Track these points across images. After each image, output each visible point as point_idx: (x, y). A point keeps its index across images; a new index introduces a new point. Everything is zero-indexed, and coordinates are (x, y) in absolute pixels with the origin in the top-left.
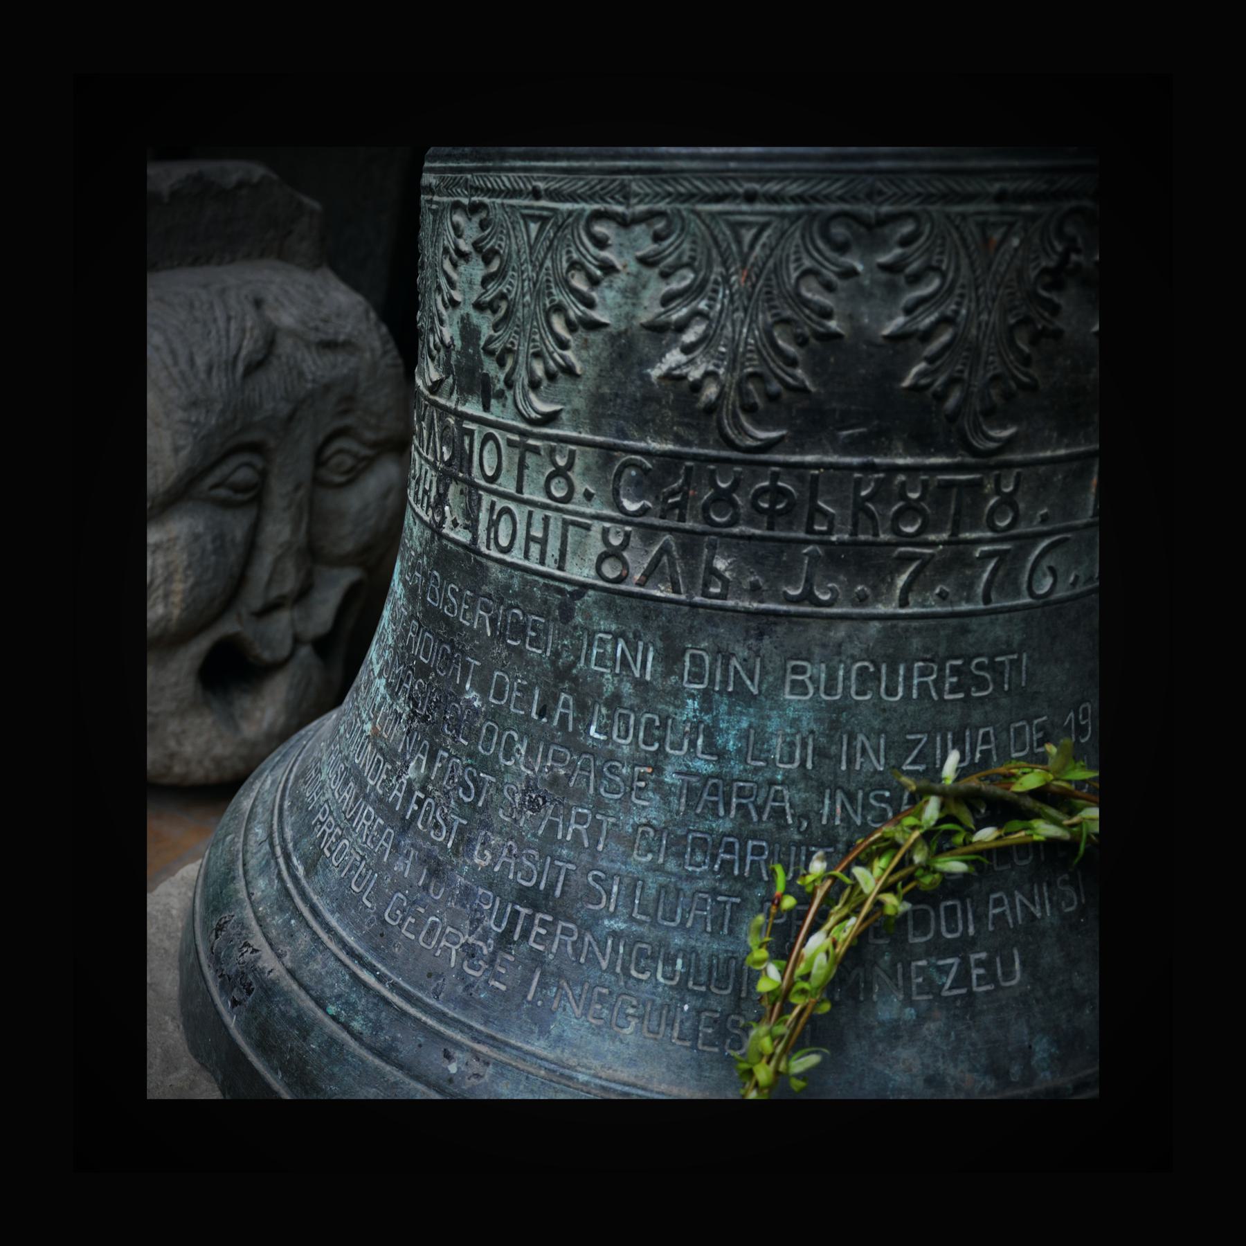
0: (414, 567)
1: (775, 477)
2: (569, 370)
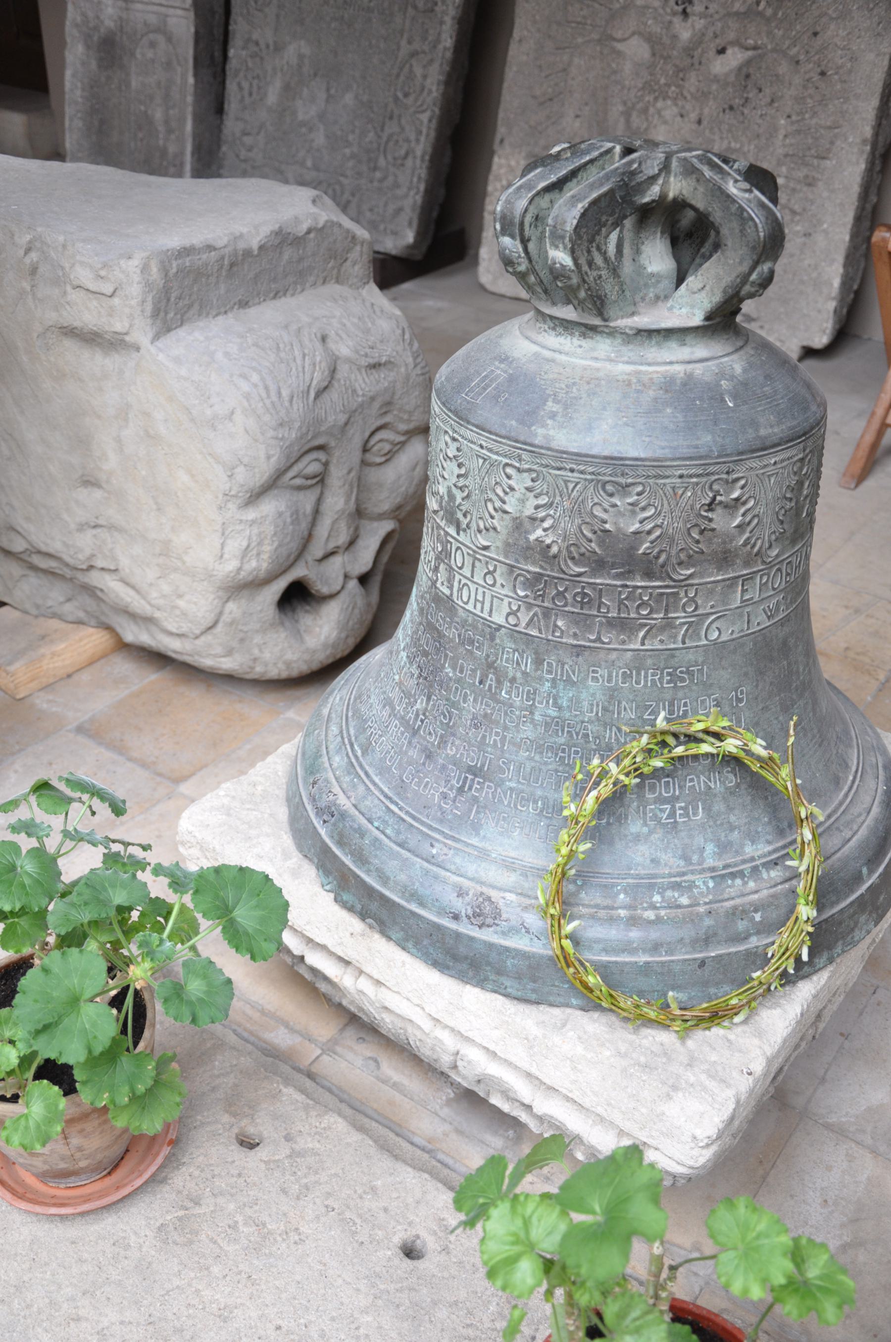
0: (422, 597)
1: (583, 588)
2: (495, 529)
